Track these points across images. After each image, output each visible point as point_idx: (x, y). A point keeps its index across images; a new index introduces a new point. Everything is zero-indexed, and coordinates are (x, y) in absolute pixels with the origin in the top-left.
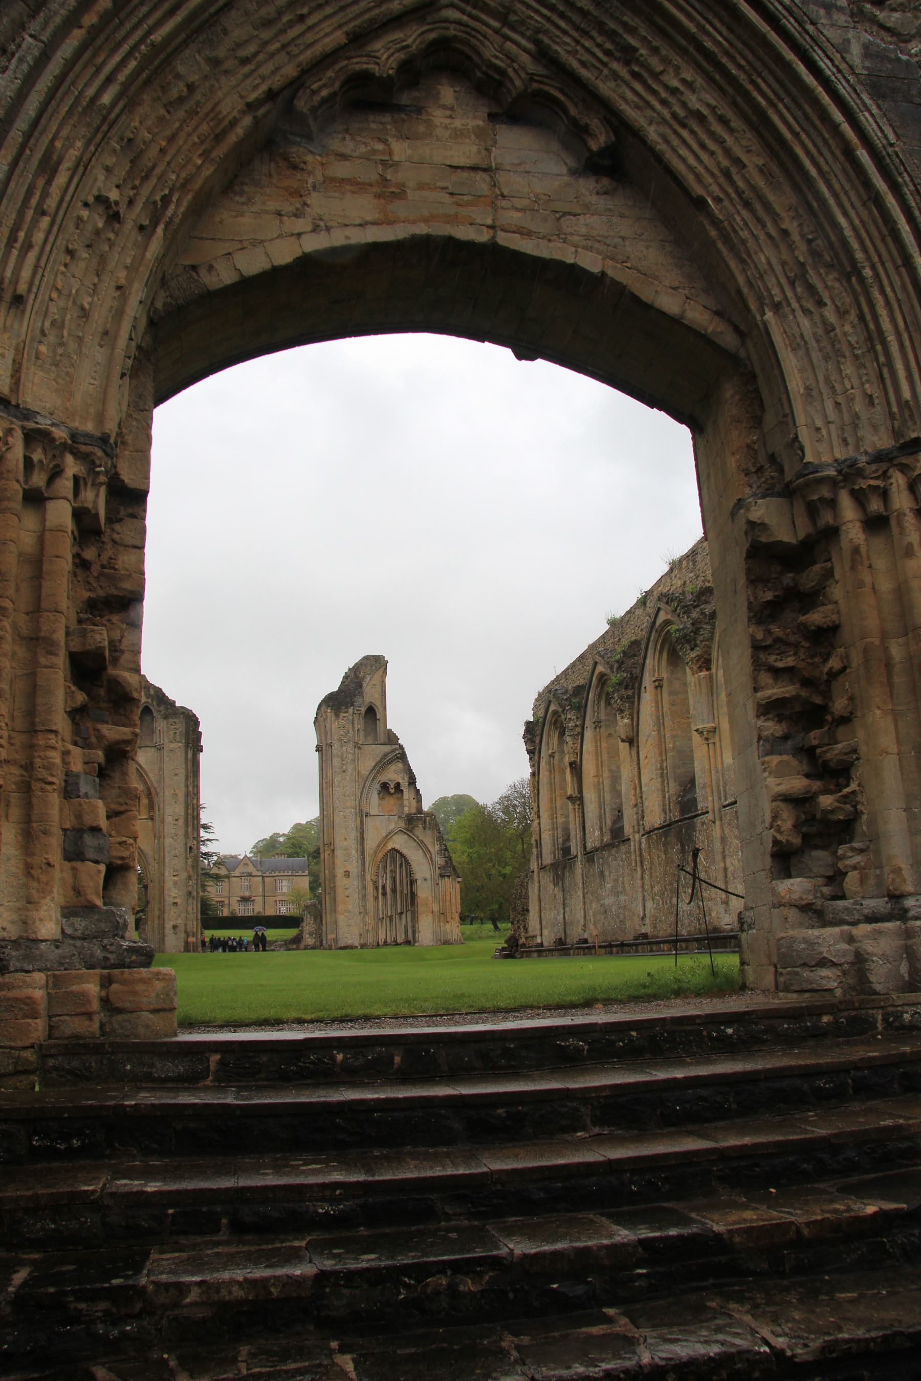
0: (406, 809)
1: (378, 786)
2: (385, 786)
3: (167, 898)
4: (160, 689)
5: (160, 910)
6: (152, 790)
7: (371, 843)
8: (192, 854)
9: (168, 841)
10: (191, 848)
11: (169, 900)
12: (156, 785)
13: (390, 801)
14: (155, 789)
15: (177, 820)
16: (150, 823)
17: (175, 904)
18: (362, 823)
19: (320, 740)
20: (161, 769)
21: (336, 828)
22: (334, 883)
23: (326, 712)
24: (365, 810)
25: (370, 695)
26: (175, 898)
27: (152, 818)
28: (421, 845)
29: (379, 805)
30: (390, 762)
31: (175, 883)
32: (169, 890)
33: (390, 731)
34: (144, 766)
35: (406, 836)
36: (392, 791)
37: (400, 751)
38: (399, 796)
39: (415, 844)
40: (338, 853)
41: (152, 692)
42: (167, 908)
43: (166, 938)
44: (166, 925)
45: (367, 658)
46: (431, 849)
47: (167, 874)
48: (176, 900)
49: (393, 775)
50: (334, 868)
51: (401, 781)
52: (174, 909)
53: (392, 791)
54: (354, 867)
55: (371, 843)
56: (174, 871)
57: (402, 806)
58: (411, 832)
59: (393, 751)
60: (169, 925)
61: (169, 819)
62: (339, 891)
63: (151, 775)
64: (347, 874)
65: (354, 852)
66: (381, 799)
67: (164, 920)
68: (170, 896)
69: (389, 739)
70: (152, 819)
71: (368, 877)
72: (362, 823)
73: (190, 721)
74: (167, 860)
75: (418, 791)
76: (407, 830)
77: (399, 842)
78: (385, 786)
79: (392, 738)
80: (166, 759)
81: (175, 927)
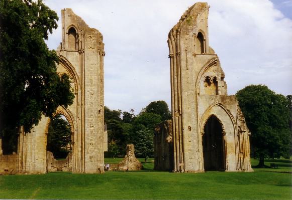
0: (219, 92)
1: (204, 79)
7: (202, 110)
18: (196, 99)
24: (198, 92)
25: (199, 26)
26: (91, 140)
28: (228, 112)
30: (211, 65)
31: (92, 132)
37: (217, 59)
40: (185, 116)
46: (234, 115)
48: (92, 142)
49: (212, 73)
52: (91, 147)
54: (193, 124)
55: (202, 110)
57: (217, 91)
64: (190, 128)
65: (193, 115)
71: (199, 131)
72: (196, 99)
73: (100, 37)
75: (225, 83)
77: (216, 111)
78: (208, 80)
79: (212, 53)
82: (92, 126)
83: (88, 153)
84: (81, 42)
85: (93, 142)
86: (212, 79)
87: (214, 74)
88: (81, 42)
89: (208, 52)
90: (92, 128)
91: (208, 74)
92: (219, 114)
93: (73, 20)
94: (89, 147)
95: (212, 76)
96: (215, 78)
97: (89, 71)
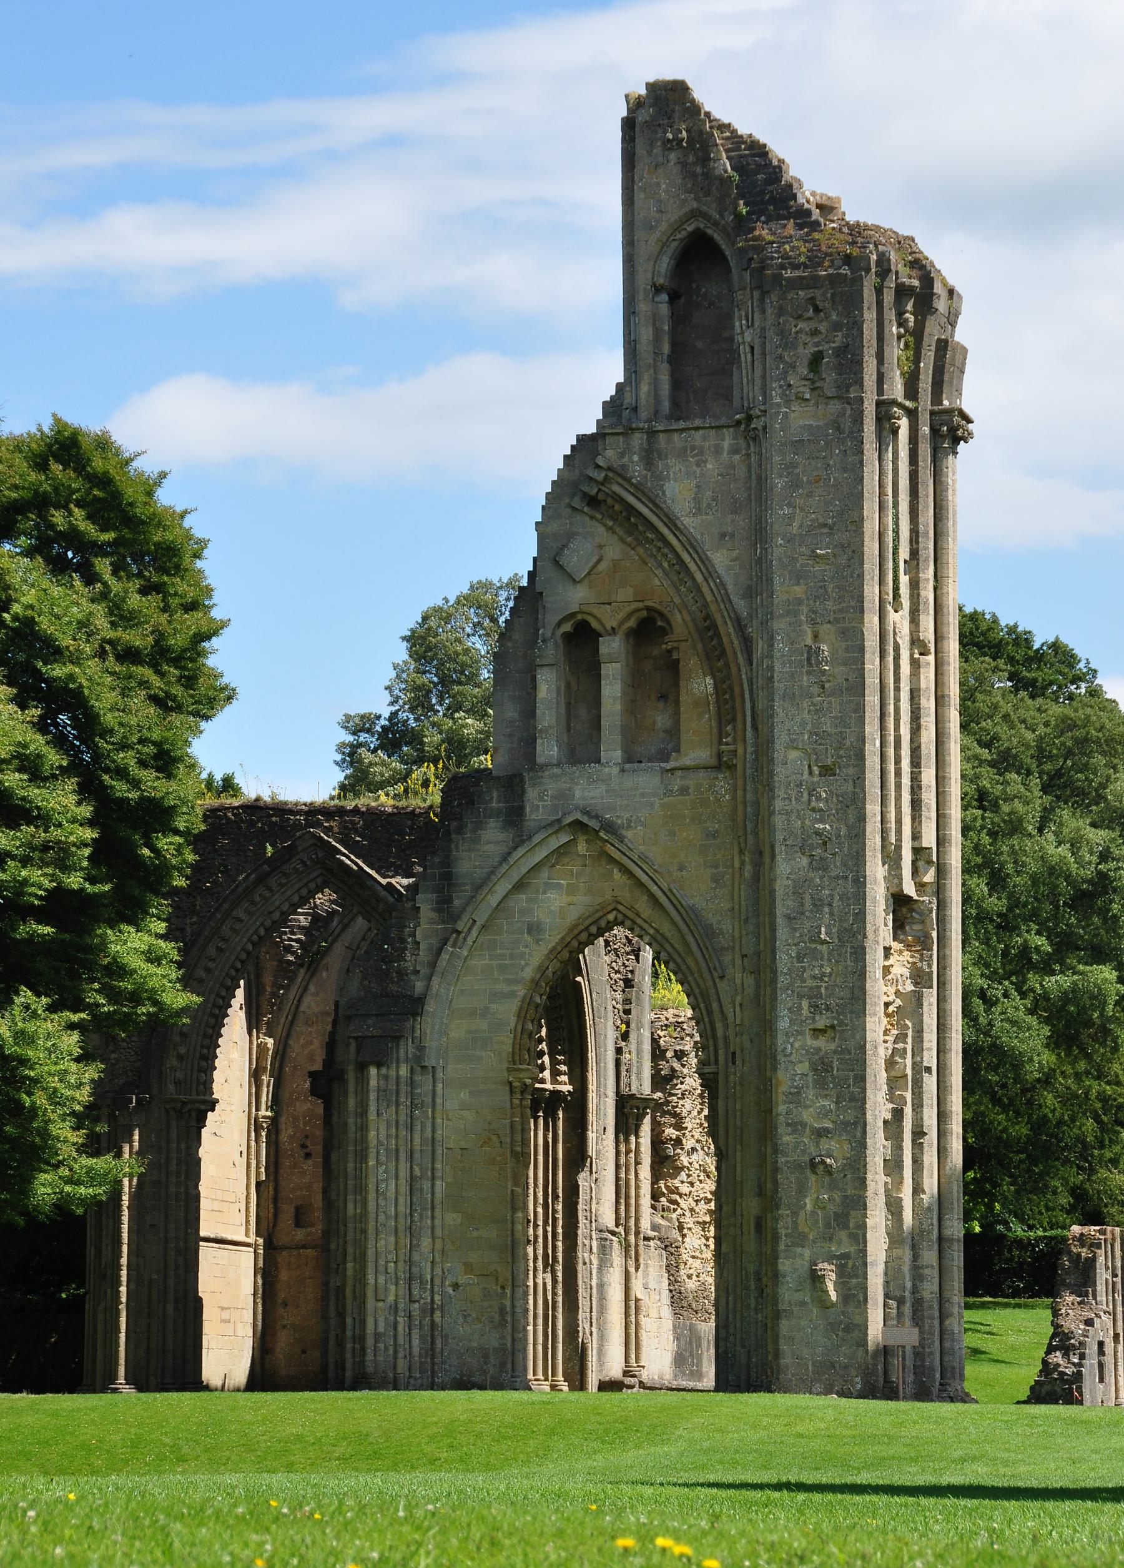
3: (786, 1138)
4: (759, 150)
5: (761, 1192)
6: (728, 631)
12: (741, 605)
14: (740, 626)
16: (722, 785)
20: (759, 534)
26: (821, 1133)
27: (721, 764)
31: (821, 1067)
32: (796, 1097)
34: (689, 522)
42: (787, 1180)
43: (785, 1326)
44: (784, 1265)
47: (783, 1024)
63: (720, 559)
67: (776, 1238)
68: (797, 1126)
70: (732, 767)
74: (784, 959)
80: (779, 483)
82: (822, 1022)
83: (800, 1239)
84: (752, 348)
88: (752, 348)
90: (821, 1043)
94: (802, 1191)
97: (799, 577)
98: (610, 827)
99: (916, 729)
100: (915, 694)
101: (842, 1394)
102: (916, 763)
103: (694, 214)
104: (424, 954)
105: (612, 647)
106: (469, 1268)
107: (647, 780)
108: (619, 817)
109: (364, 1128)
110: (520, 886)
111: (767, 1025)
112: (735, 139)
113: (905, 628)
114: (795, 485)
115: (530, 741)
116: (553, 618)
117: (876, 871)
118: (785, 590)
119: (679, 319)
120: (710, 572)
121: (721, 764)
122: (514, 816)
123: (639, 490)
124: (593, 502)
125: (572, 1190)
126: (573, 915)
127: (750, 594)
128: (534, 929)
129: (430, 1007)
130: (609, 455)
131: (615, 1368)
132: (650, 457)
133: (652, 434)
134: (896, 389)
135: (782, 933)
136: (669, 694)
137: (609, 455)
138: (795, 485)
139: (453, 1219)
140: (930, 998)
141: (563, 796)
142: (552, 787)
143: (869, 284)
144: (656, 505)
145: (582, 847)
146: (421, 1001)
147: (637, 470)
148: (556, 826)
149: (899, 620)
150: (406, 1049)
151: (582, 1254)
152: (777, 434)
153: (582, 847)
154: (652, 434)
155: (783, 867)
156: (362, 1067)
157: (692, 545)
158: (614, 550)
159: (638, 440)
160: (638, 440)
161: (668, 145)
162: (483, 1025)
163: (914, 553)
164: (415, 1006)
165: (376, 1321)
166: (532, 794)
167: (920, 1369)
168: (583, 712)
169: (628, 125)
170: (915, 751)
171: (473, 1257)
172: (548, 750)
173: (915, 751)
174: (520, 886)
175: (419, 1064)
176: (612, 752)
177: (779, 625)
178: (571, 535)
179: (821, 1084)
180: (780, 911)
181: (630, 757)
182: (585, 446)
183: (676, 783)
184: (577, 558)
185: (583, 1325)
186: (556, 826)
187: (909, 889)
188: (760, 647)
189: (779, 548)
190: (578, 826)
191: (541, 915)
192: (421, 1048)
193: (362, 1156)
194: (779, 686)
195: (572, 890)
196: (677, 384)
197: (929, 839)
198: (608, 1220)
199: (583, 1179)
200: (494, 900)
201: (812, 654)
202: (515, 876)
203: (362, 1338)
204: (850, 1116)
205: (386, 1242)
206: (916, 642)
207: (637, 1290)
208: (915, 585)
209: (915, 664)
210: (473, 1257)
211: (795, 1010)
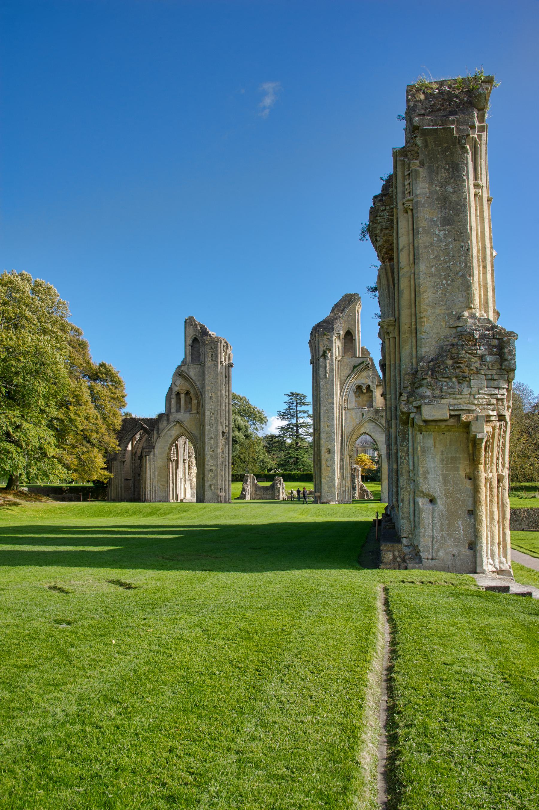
2: (359, 388)
3: (206, 466)
5: (203, 474)
6: (199, 393)
8: (225, 437)
9: (207, 428)
10: (223, 432)
11: (207, 468)
12: (201, 390)
13: (365, 398)
15: (213, 414)
16: (198, 416)
17: (211, 470)
19: (312, 357)
20: (204, 380)
21: (322, 419)
22: (320, 457)
23: (315, 336)
26: (211, 466)
27: (198, 413)
29: (356, 401)
31: (212, 456)
32: (208, 461)
33: (362, 349)
34: (193, 378)
35: (374, 424)
36: (365, 391)
38: (371, 394)
39: (380, 430)
41: (199, 328)
42: (206, 472)
43: (206, 493)
44: (206, 484)
45: (346, 296)
47: (206, 450)
50: (320, 446)
51: (371, 384)
53: (365, 391)
56: (211, 448)
58: (377, 420)
59: (363, 362)
60: (207, 484)
61: (207, 413)
62: (323, 462)
63: (198, 383)
66: (356, 397)
68: (208, 465)
69: (362, 354)
71: (345, 453)
74: (207, 440)
76: (375, 419)
78: (359, 388)
80: (206, 373)
81: (210, 486)
82: (212, 450)
83: (208, 481)
85: (214, 468)
86: (364, 388)
87: (368, 382)
89: (357, 356)
90: (212, 453)
91: (358, 382)
92: (373, 432)
93: (195, 330)
94: (209, 474)
95: (364, 384)
96: (368, 387)
97: (209, 386)
98: (182, 422)
99: (226, 408)
100: (225, 403)
101: (214, 503)
102: (225, 413)
103: (195, 335)
104: (155, 440)
105: (182, 396)
106: (161, 484)
107: (187, 415)
108: (183, 420)
109: (146, 465)
110: (169, 430)
111: (204, 450)
112: (200, 325)
113: (224, 393)
114: (209, 373)
115: (170, 409)
116: (174, 392)
117: (220, 428)
118: (207, 388)
119: (192, 349)
120: (196, 386)
121: (198, 413)
122: (168, 420)
123: (186, 373)
124: (180, 375)
125: (176, 473)
126: (176, 434)
127: (202, 388)
128: (171, 436)
129: (156, 447)
130: (182, 368)
131: (182, 497)
132: (188, 369)
133: (188, 365)
134: (223, 359)
135: (206, 437)
136: (190, 403)
137: (182, 368)
138: (209, 373)
139: (159, 477)
140: (227, 446)
141: (175, 417)
142: (174, 416)
143: (219, 344)
144: (188, 375)
145: (178, 425)
146: (154, 446)
147: (186, 371)
148: (174, 421)
149: (223, 393)
150: (152, 453)
151: (178, 482)
152: (206, 366)
153: (178, 425)
154: (188, 365)
155: (207, 428)
156: (146, 456)
157: (194, 382)
158: (183, 382)
159: (186, 366)
160: (186, 366)
161: (191, 325)
162: (163, 450)
163: (226, 383)
164: (153, 447)
165: (148, 492)
166: (170, 417)
167: (225, 499)
168: (178, 405)
169: (186, 322)
170: (225, 411)
171: (162, 483)
172: (173, 410)
173: (225, 411)
174: (169, 430)
175: (154, 455)
176: (182, 411)
177: (206, 393)
178: (177, 380)
179: (211, 459)
180: (206, 434)
181: (185, 412)
182: (179, 367)
183: (191, 415)
184: (178, 383)
185: (178, 492)
186: (174, 421)
187: (225, 431)
188: (203, 396)
189: (206, 382)
190: (177, 421)
191: (172, 434)
192: (154, 453)
193: (146, 468)
194: (206, 402)
195: (176, 431)
196: (192, 359)
197: (227, 424)
198: (182, 477)
199: (178, 471)
200: (165, 432)
201: (211, 397)
202: (168, 429)
203: (145, 494)
204: (216, 463)
205: (149, 481)
206: (226, 395)
207: (186, 486)
208: (226, 387)
209: (226, 399)
210: (162, 483)
211: (208, 448)
